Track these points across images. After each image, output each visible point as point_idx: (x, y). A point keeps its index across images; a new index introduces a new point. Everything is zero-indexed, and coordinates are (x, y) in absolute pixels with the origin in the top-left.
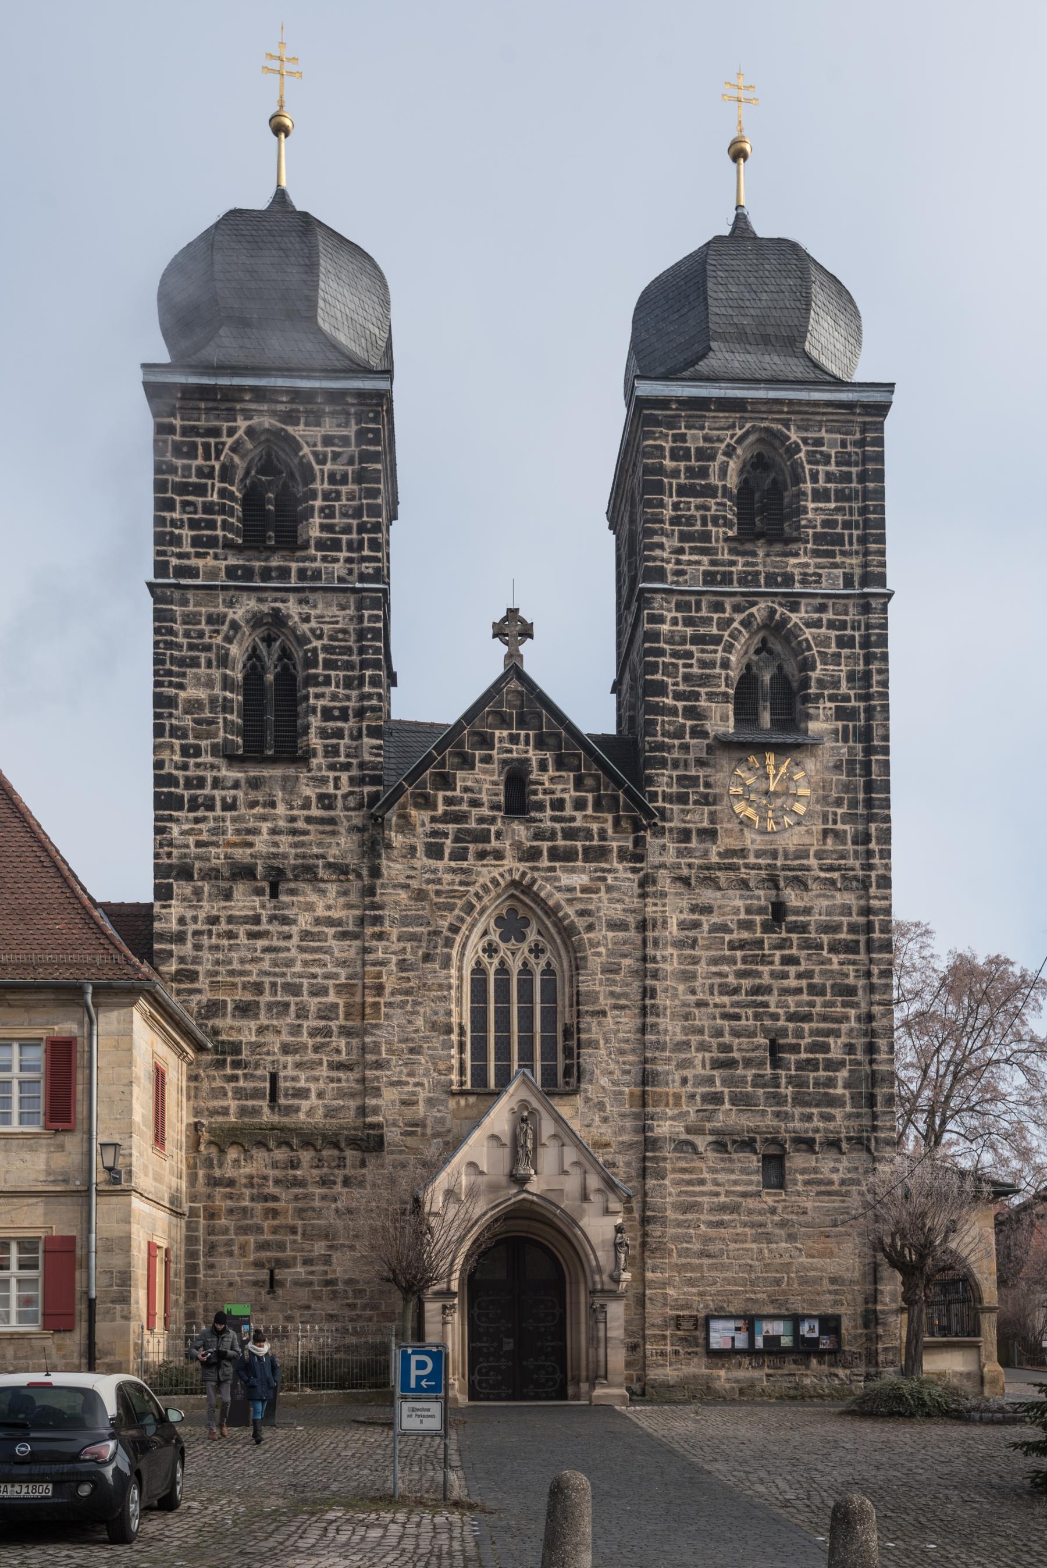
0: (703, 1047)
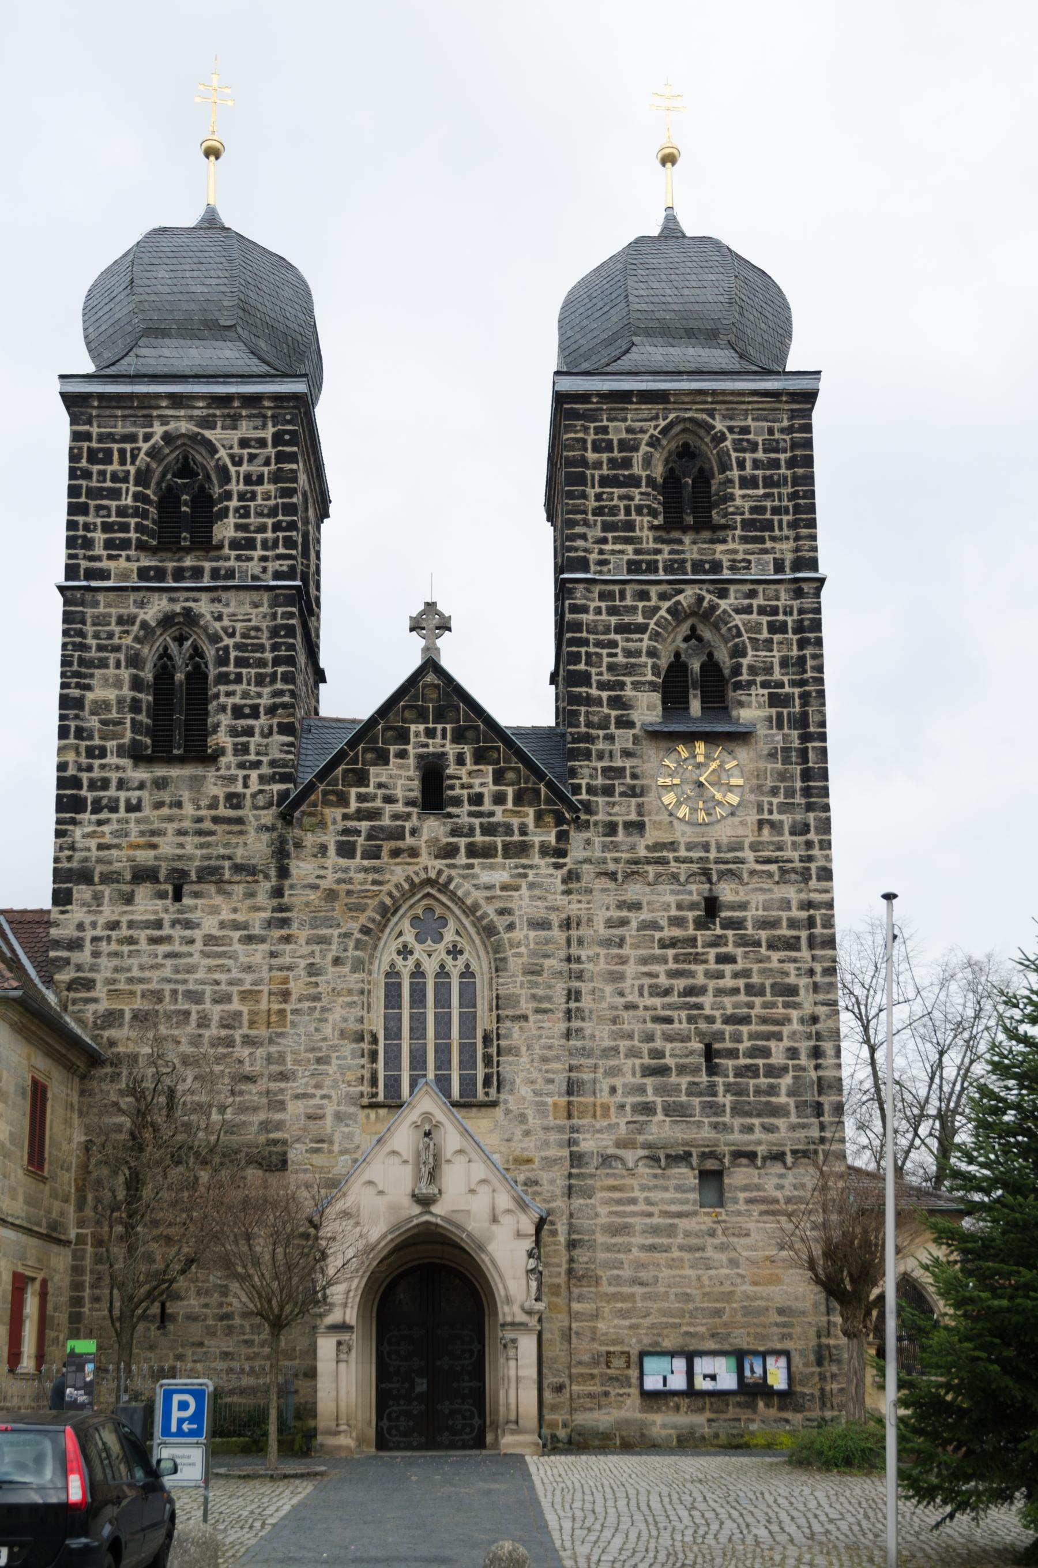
0: (633, 1053)
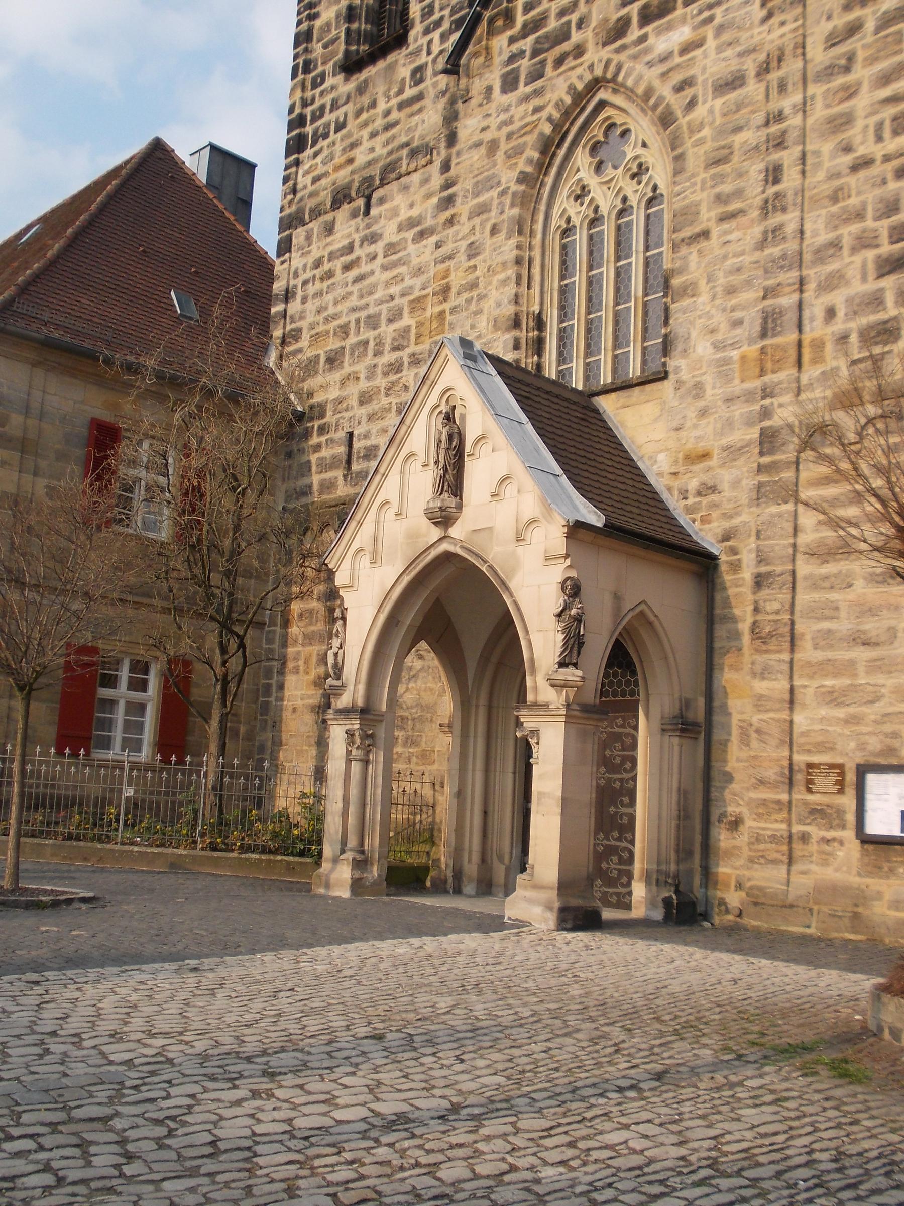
0: (864, 242)
